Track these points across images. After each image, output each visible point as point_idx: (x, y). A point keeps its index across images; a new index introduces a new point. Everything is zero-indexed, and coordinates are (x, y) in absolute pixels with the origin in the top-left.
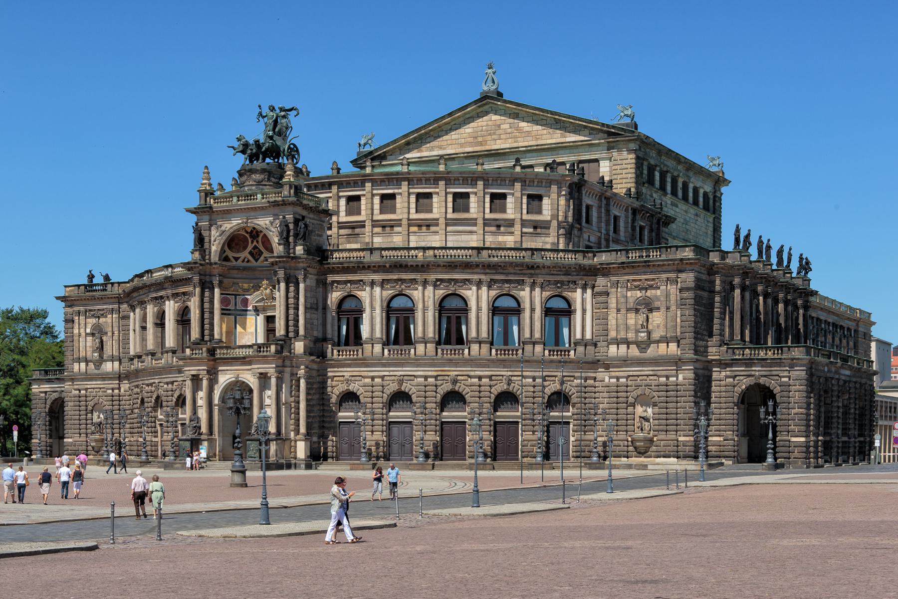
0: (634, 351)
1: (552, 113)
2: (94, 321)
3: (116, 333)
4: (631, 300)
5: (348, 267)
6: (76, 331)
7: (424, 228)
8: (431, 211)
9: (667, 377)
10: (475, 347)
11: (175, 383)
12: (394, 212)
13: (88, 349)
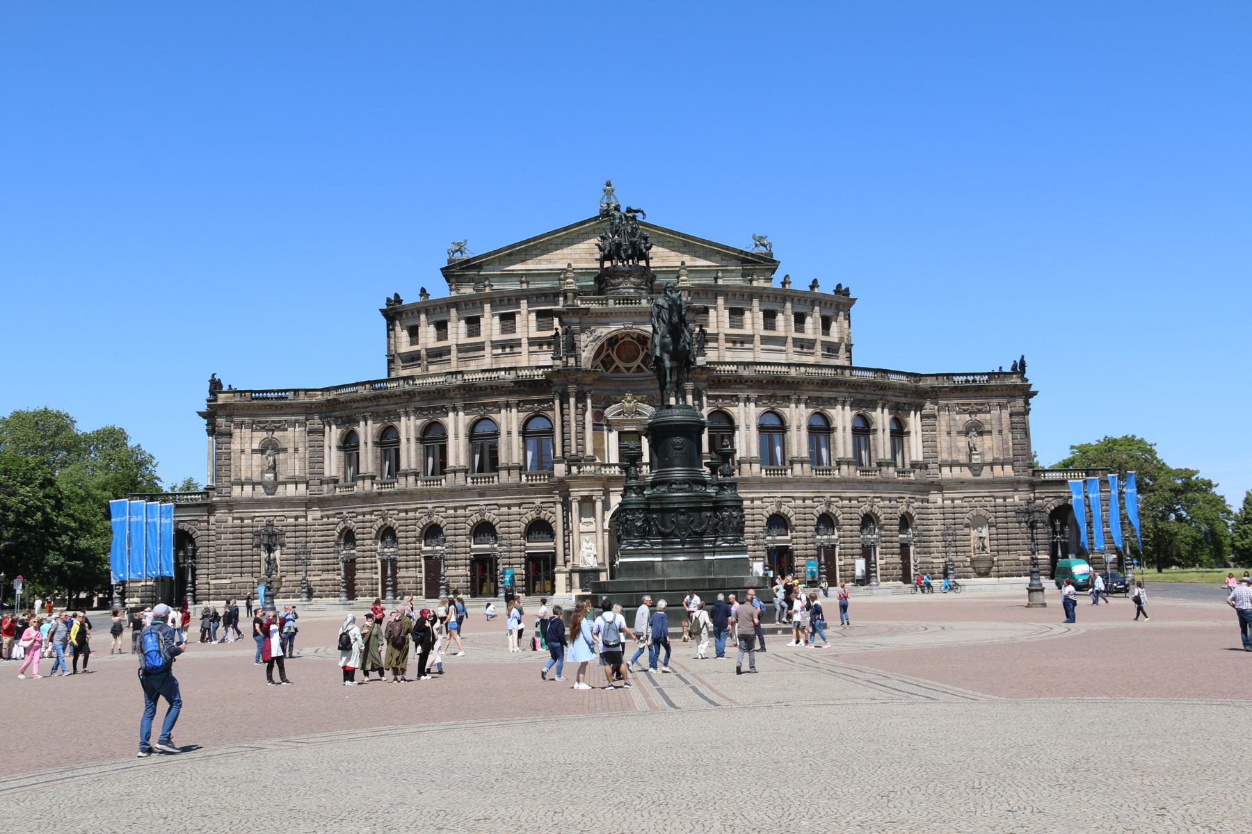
0: (967, 474)
1: (684, 236)
2: (264, 434)
3: (301, 449)
6: (236, 446)
8: (741, 327)
9: (1005, 498)
10: (844, 468)
13: (254, 469)
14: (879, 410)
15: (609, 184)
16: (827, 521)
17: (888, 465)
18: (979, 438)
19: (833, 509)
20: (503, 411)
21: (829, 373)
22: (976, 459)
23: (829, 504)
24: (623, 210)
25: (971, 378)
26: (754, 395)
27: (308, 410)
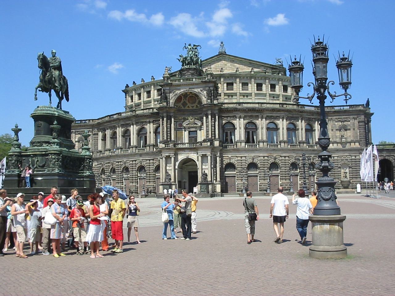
0: (340, 146)
1: (249, 60)
2: (79, 136)
4: (338, 126)
5: (230, 110)
7: (246, 97)
8: (248, 90)
9: (355, 156)
11: (137, 161)
12: (233, 90)
14: (300, 121)
15: (222, 43)
16: (274, 166)
17: (303, 143)
18: (345, 132)
19: (277, 161)
20: (148, 124)
21: (277, 106)
22: (344, 140)
23: (275, 159)
24: (192, 46)
25: (342, 108)
26: (243, 115)
27: (93, 127)
